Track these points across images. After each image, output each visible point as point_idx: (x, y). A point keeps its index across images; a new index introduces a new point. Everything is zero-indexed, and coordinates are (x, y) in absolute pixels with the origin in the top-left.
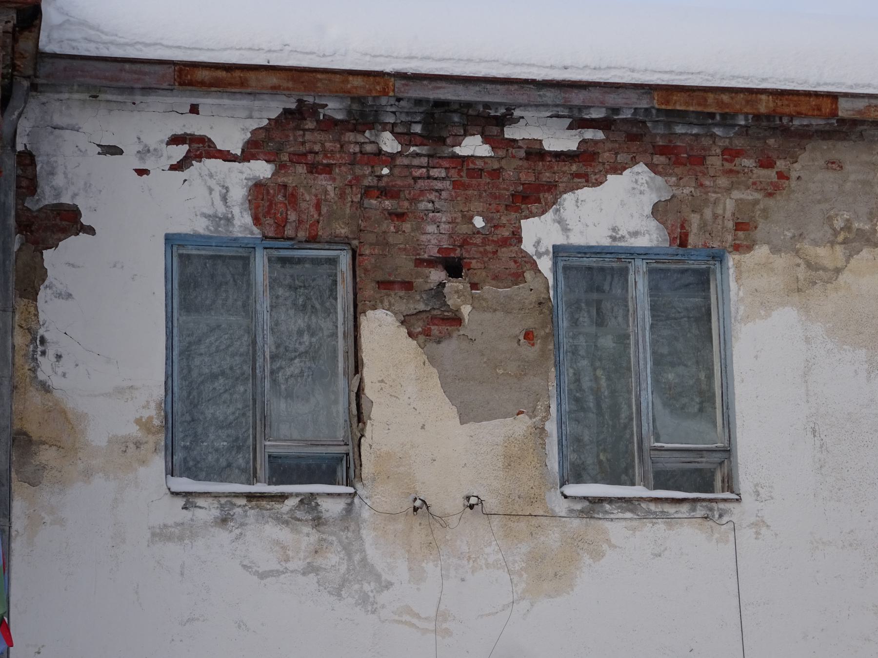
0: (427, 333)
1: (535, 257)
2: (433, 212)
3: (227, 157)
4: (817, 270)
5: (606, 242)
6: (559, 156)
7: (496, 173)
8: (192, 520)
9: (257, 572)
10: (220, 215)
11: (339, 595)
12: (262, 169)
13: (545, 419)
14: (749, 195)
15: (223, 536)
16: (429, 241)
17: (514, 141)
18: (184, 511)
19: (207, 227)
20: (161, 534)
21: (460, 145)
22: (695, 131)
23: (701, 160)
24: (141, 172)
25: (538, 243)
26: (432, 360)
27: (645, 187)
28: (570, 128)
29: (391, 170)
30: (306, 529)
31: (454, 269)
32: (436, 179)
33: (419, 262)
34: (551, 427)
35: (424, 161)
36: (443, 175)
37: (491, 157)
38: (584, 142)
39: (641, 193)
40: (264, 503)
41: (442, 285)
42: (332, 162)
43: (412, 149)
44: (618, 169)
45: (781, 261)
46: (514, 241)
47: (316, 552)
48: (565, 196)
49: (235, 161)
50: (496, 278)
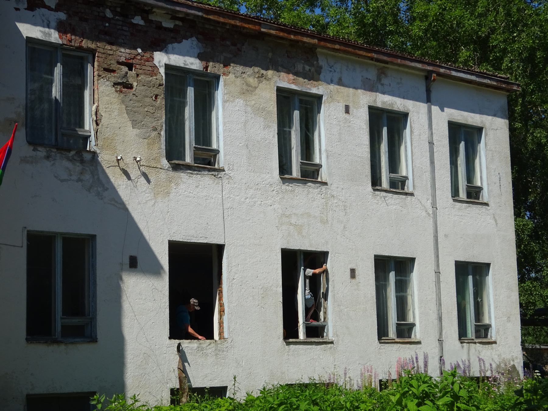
0: (121, 91)
1: (158, 67)
2: (123, 44)
3: (49, 8)
4: (249, 87)
5: (182, 65)
6: (166, 29)
8: (36, 155)
9: (60, 179)
10: (46, 32)
11: (89, 191)
12: (62, 16)
13: (161, 130)
16: (122, 55)
17: (152, 21)
18: (33, 152)
19: (42, 36)
21: (133, 19)
22: (212, 28)
24: (17, 9)
25: (159, 62)
26: (123, 102)
27: (195, 46)
28: (171, 19)
29: (109, 24)
30: (78, 164)
31: (130, 67)
32: (125, 31)
33: (119, 63)
34: (163, 133)
35: (121, 23)
36: (127, 30)
37: (144, 25)
38: (175, 25)
39: (194, 48)
40: (63, 152)
41: (127, 73)
42: (88, 17)
43: (117, 17)
45: (239, 81)
46: (151, 59)
47: (81, 173)
48: (169, 45)
49: (52, 11)
50: (145, 74)
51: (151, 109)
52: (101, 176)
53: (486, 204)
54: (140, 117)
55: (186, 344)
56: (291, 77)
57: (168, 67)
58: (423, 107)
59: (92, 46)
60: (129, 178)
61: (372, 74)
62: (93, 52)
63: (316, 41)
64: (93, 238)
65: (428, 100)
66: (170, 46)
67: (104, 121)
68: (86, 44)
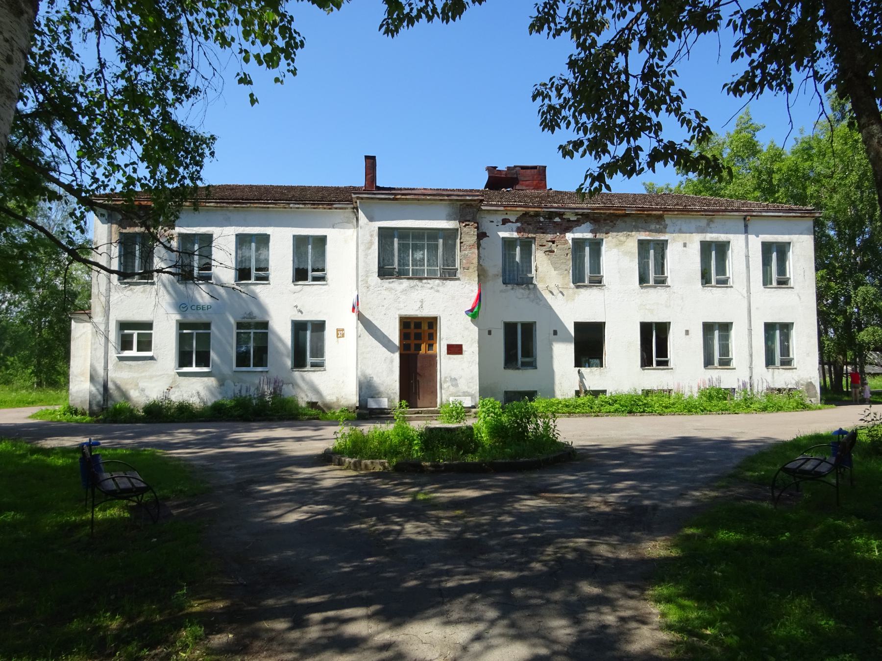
3: (513, 222)
7: (561, 225)
12: (519, 224)
14: (608, 228)
15: (513, 292)
20: (501, 291)
23: (599, 221)
31: (553, 242)
34: (571, 271)
44: (584, 223)
45: (614, 240)
51: (564, 261)
52: (539, 295)
53: (793, 288)
54: (559, 265)
55: (583, 370)
56: (647, 233)
57: (573, 239)
58: (742, 237)
59: (534, 236)
60: (553, 294)
61: (703, 222)
62: (534, 238)
63: (661, 212)
64: (535, 322)
65: (746, 232)
66: (575, 229)
67: (539, 270)
68: (530, 235)
